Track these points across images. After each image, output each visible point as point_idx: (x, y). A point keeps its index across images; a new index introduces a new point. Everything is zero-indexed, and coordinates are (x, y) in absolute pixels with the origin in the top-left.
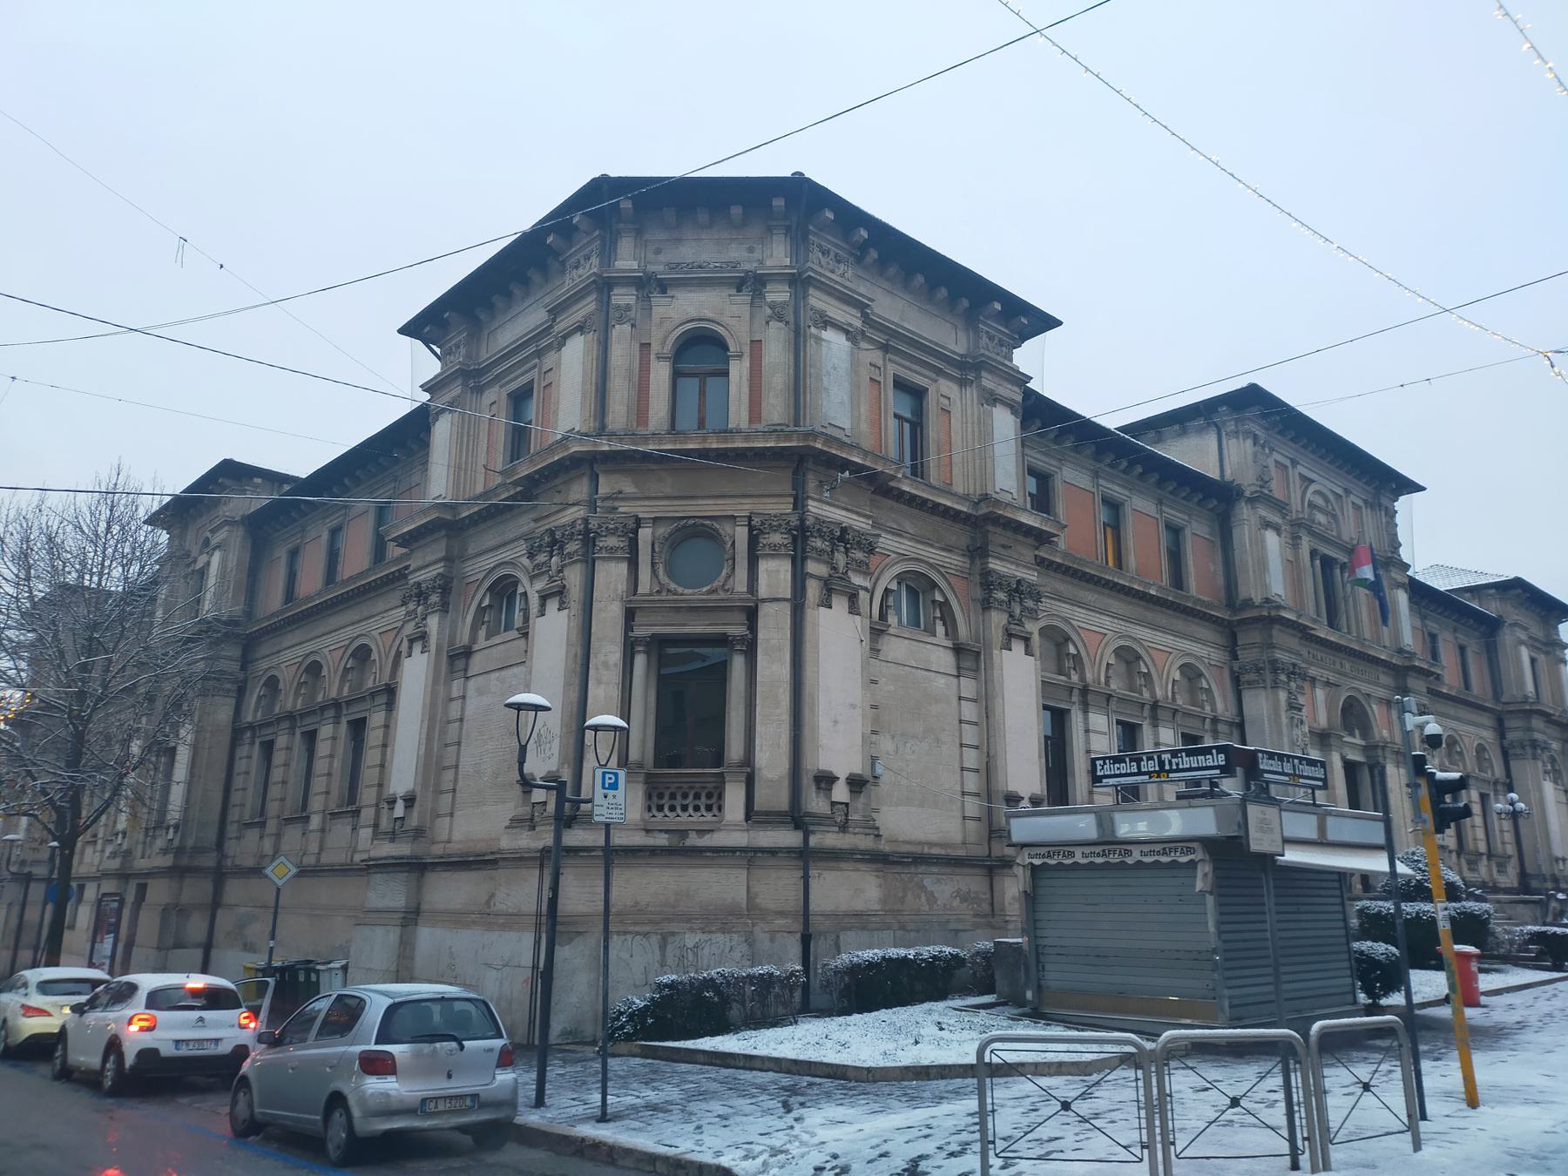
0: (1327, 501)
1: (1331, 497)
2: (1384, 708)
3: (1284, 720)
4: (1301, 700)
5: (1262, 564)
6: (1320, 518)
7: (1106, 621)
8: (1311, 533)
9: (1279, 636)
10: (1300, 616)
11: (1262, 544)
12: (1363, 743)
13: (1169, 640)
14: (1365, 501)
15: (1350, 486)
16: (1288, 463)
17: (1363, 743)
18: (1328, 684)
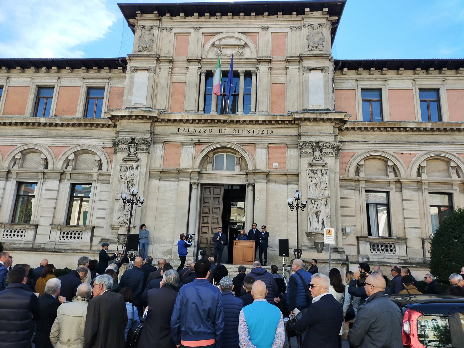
0: (241, 40)
1: (242, 36)
2: (281, 150)
3: (119, 168)
4: (140, 156)
5: (131, 91)
6: (229, 52)
7: (17, 140)
8: (200, 62)
9: (123, 124)
10: (132, 112)
11: (132, 81)
12: (242, 173)
13: (68, 141)
14: (291, 28)
15: (270, 24)
16: (192, 31)
17: (242, 173)
18: (199, 143)
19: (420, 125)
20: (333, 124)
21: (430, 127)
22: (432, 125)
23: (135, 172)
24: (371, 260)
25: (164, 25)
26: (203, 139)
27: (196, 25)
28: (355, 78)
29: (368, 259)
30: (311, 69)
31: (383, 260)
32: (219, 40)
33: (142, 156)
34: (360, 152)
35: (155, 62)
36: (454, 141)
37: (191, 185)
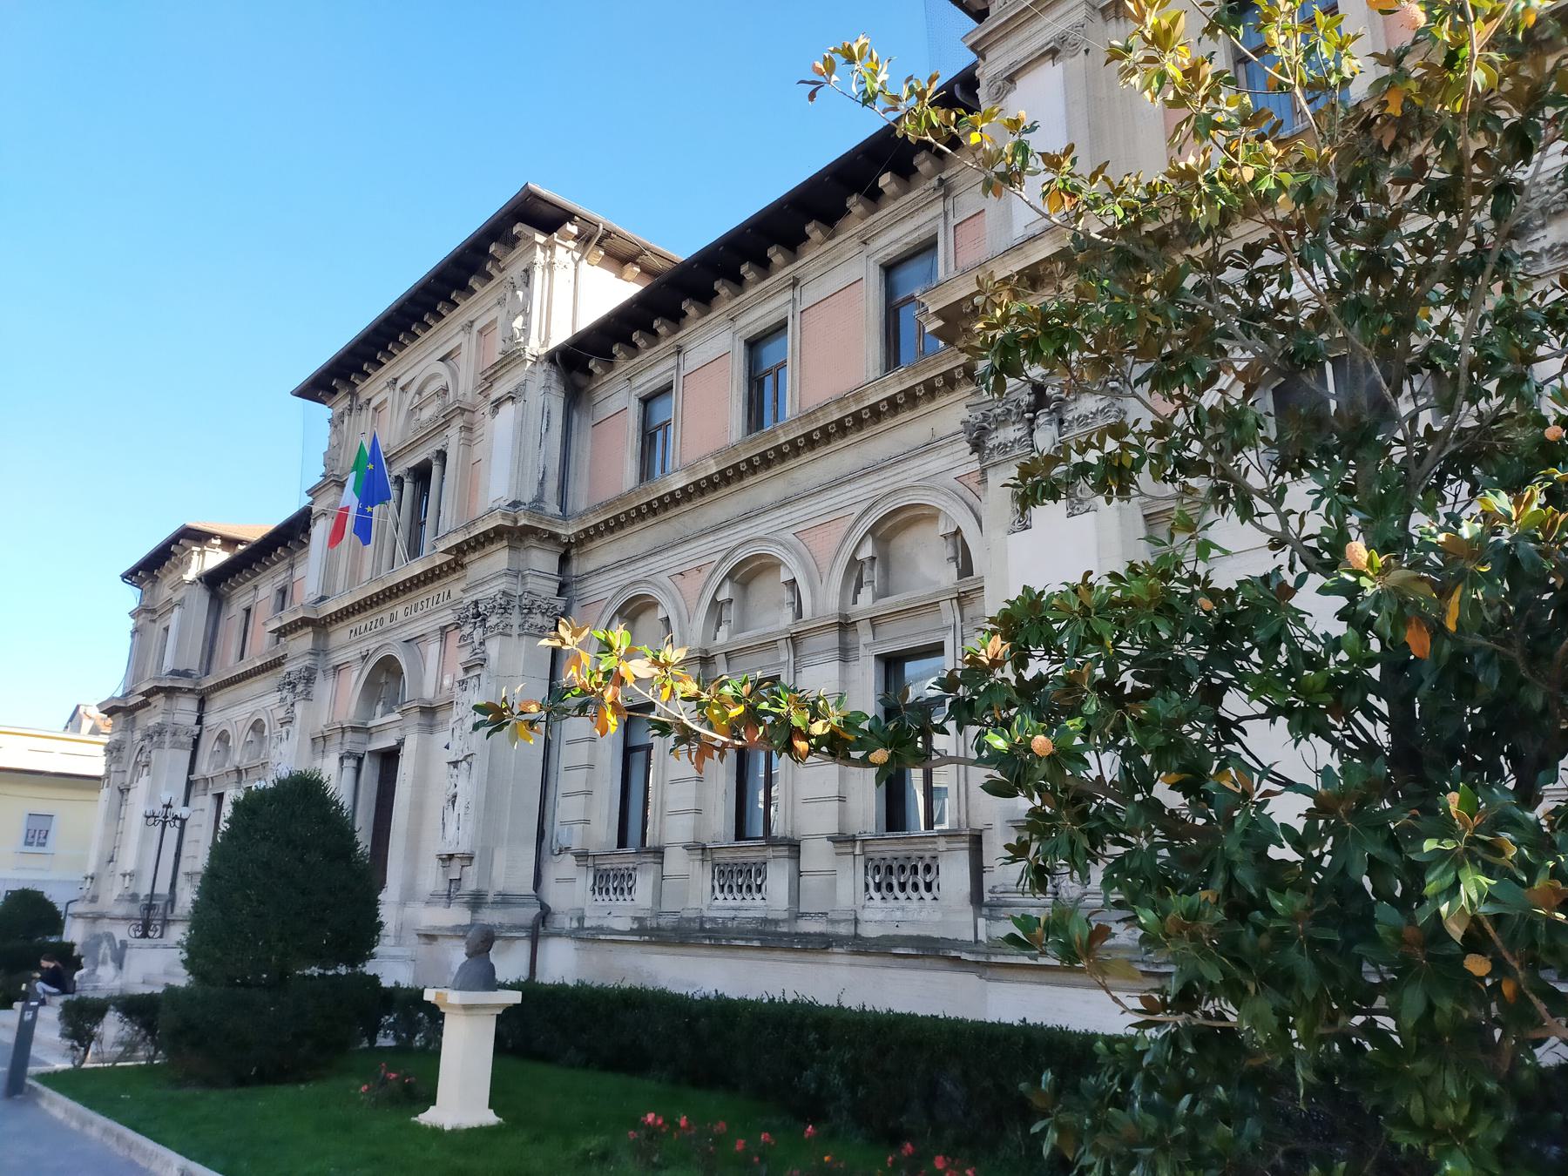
19: (695, 473)
20: (505, 543)
21: (714, 470)
22: (717, 464)
23: (283, 747)
24: (587, 924)
25: (362, 400)
26: (371, 644)
27: (388, 377)
28: (622, 378)
29: (581, 919)
30: (497, 404)
31: (606, 923)
32: (419, 392)
33: (299, 709)
34: (610, 595)
35: (335, 490)
36: (791, 491)
37: (341, 759)
